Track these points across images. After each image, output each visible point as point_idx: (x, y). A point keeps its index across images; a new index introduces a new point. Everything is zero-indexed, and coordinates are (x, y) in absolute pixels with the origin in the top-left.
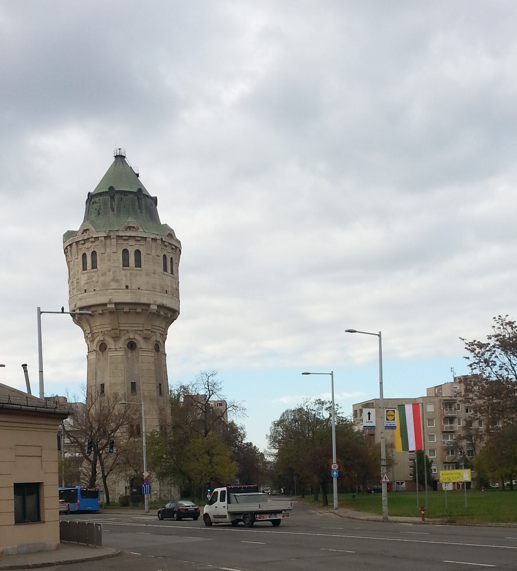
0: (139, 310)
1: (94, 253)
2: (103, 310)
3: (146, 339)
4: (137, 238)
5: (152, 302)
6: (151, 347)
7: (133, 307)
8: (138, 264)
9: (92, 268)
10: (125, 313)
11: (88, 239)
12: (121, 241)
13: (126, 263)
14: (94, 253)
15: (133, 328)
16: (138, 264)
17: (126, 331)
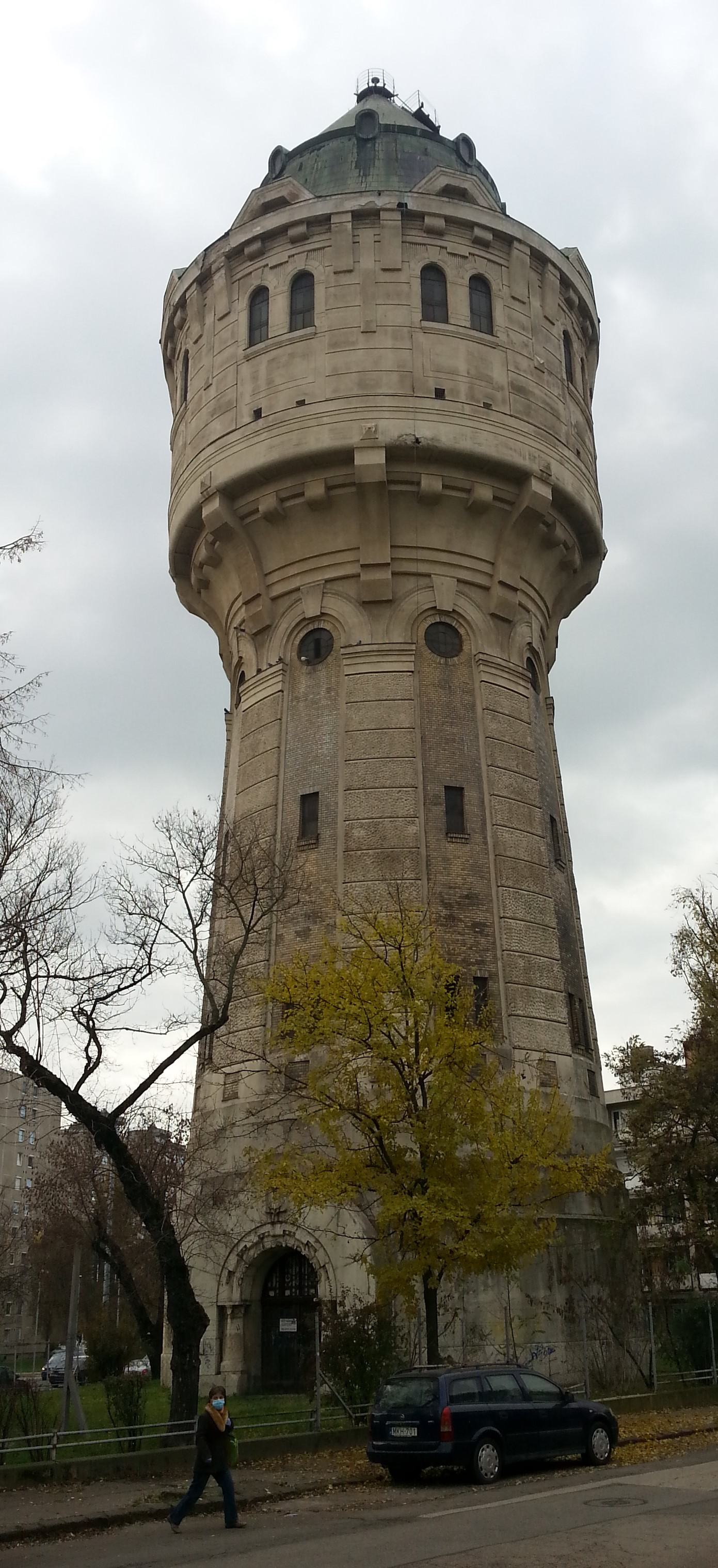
0: (484, 492)
1: (302, 282)
2: (329, 488)
3: (503, 621)
4: (477, 232)
5: (535, 467)
6: (517, 660)
7: (459, 477)
8: (483, 320)
9: (292, 330)
10: (430, 502)
11: (282, 230)
12: (416, 236)
13: (434, 307)
14: (302, 282)
15: (452, 565)
16: (483, 320)
17: (423, 582)
